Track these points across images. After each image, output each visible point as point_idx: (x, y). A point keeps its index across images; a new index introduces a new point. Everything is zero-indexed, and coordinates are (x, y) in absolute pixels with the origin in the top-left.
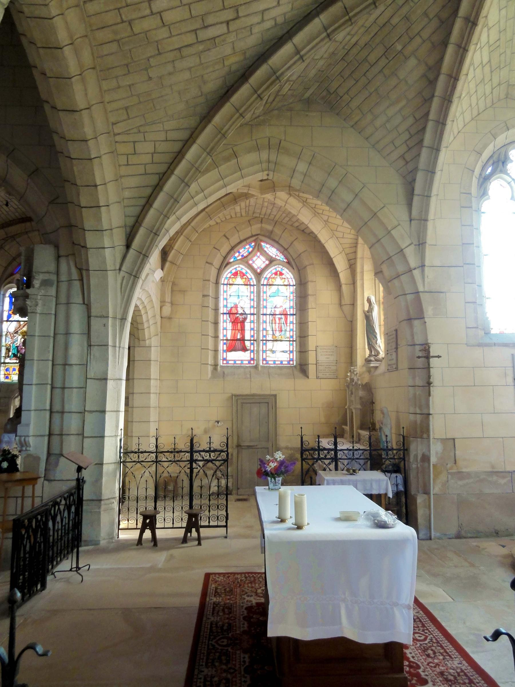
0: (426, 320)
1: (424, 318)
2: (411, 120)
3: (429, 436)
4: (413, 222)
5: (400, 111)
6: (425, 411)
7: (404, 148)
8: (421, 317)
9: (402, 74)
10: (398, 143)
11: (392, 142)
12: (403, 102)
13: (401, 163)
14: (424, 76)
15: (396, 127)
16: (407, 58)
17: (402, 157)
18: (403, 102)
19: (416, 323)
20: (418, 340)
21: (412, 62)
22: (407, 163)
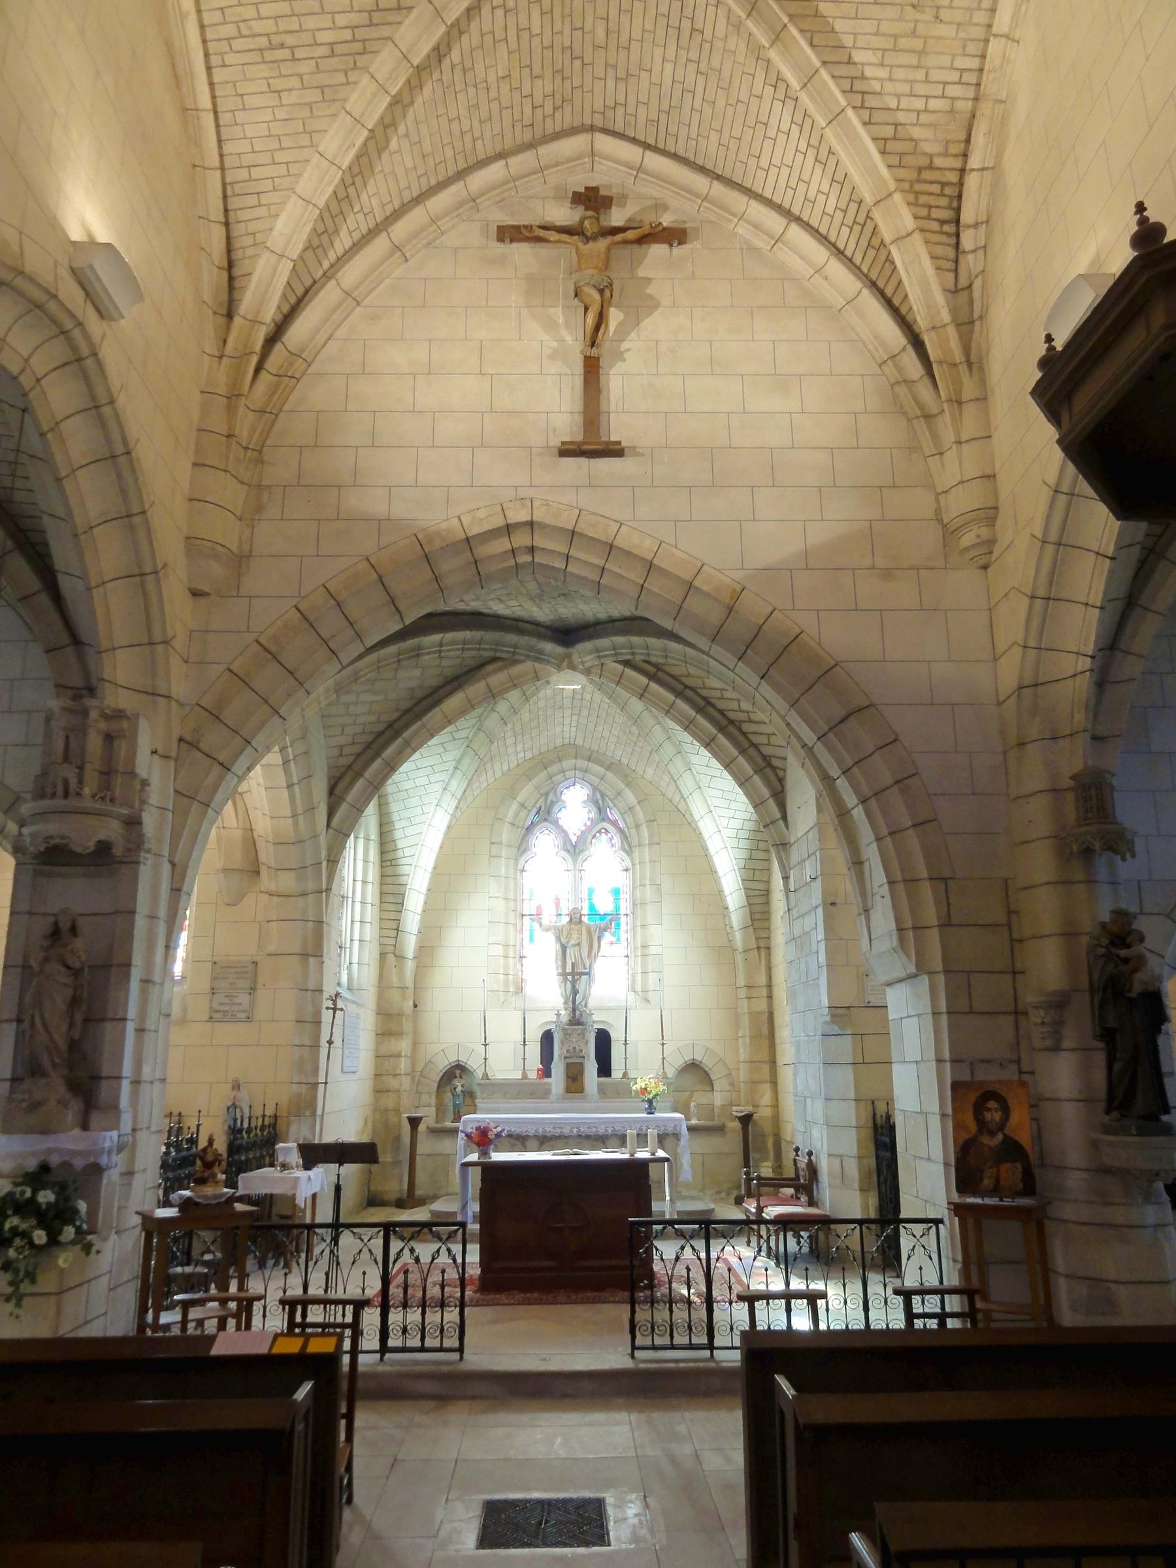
0: (325, 959)
1: (321, 956)
2: (373, 718)
3: (314, 1113)
4: (331, 831)
5: (372, 702)
6: (311, 1080)
7: (350, 740)
8: (319, 955)
9: (401, 674)
10: (349, 730)
11: (343, 727)
12: (381, 698)
13: (336, 752)
14: (413, 689)
15: (357, 715)
16: (416, 666)
17: (341, 747)
18: (381, 698)
19: (312, 960)
20: (312, 985)
21: (417, 673)
22: (341, 755)
